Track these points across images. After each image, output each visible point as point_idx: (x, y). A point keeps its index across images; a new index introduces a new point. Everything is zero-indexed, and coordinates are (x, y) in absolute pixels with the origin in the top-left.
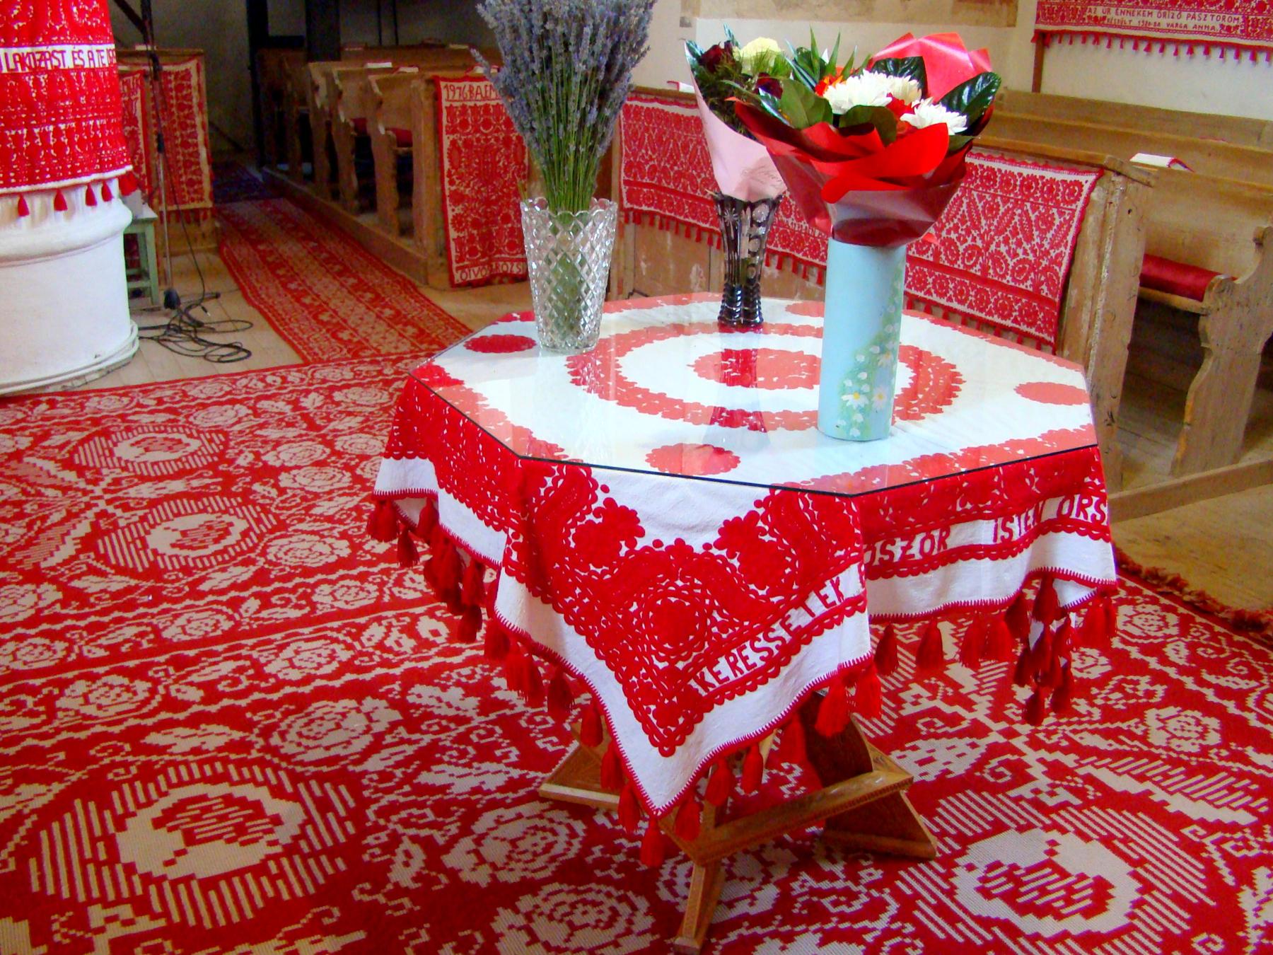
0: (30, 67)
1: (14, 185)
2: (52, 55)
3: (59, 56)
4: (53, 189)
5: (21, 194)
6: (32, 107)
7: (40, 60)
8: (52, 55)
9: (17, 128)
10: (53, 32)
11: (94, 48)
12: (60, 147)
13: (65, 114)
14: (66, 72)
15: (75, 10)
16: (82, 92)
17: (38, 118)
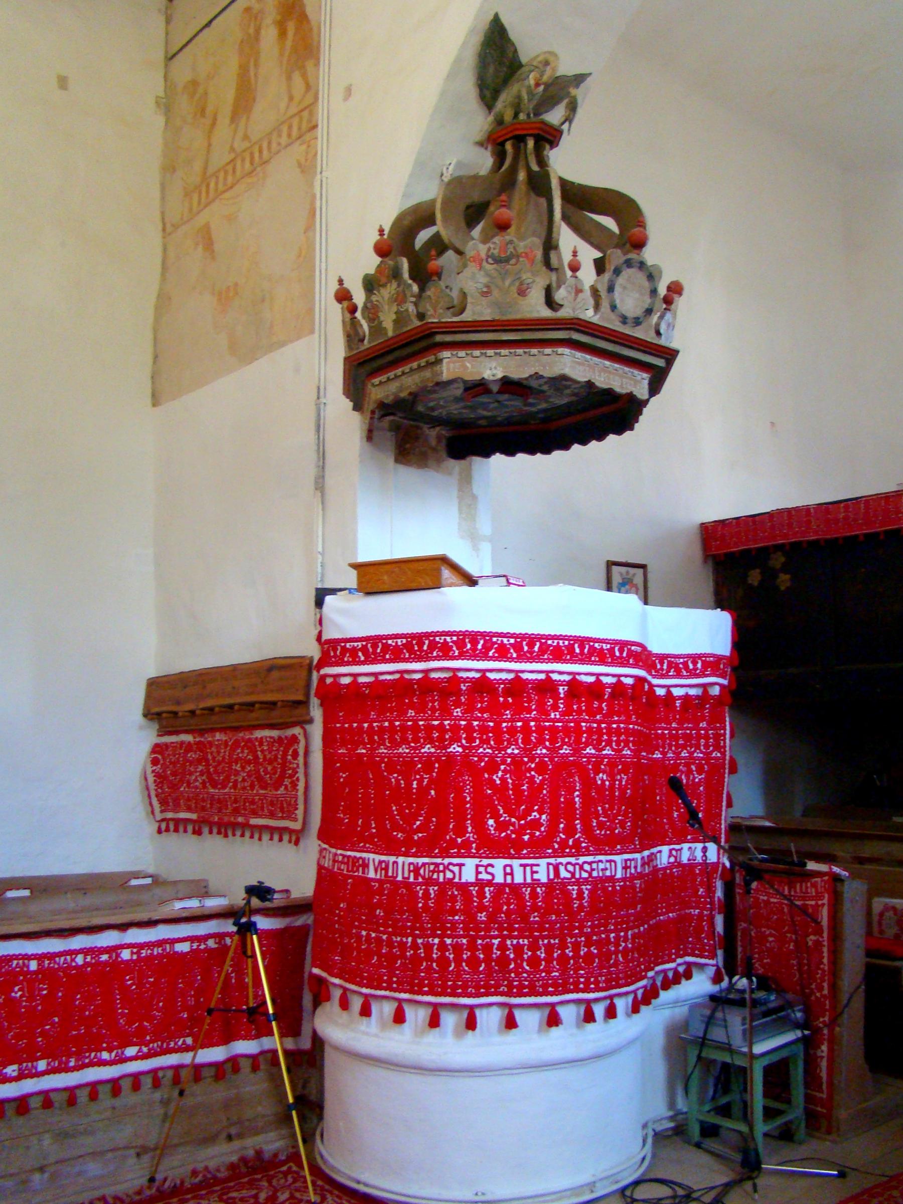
0: (423, 878)
1: (395, 990)
2: (446, 868)
3: (456, 869)
4: (429, 1004)
5: (400, 1001)
6: (417, 917)
7: (433, 872)
8: (446, 868)
9: (402, 936)
10: (453, 844)
11: (516, 863)
12: (443, 962)
13: (454, 928)
14: (464, 887)
15: (491, 822)
16: (482, 908)
17: (422, 929)
